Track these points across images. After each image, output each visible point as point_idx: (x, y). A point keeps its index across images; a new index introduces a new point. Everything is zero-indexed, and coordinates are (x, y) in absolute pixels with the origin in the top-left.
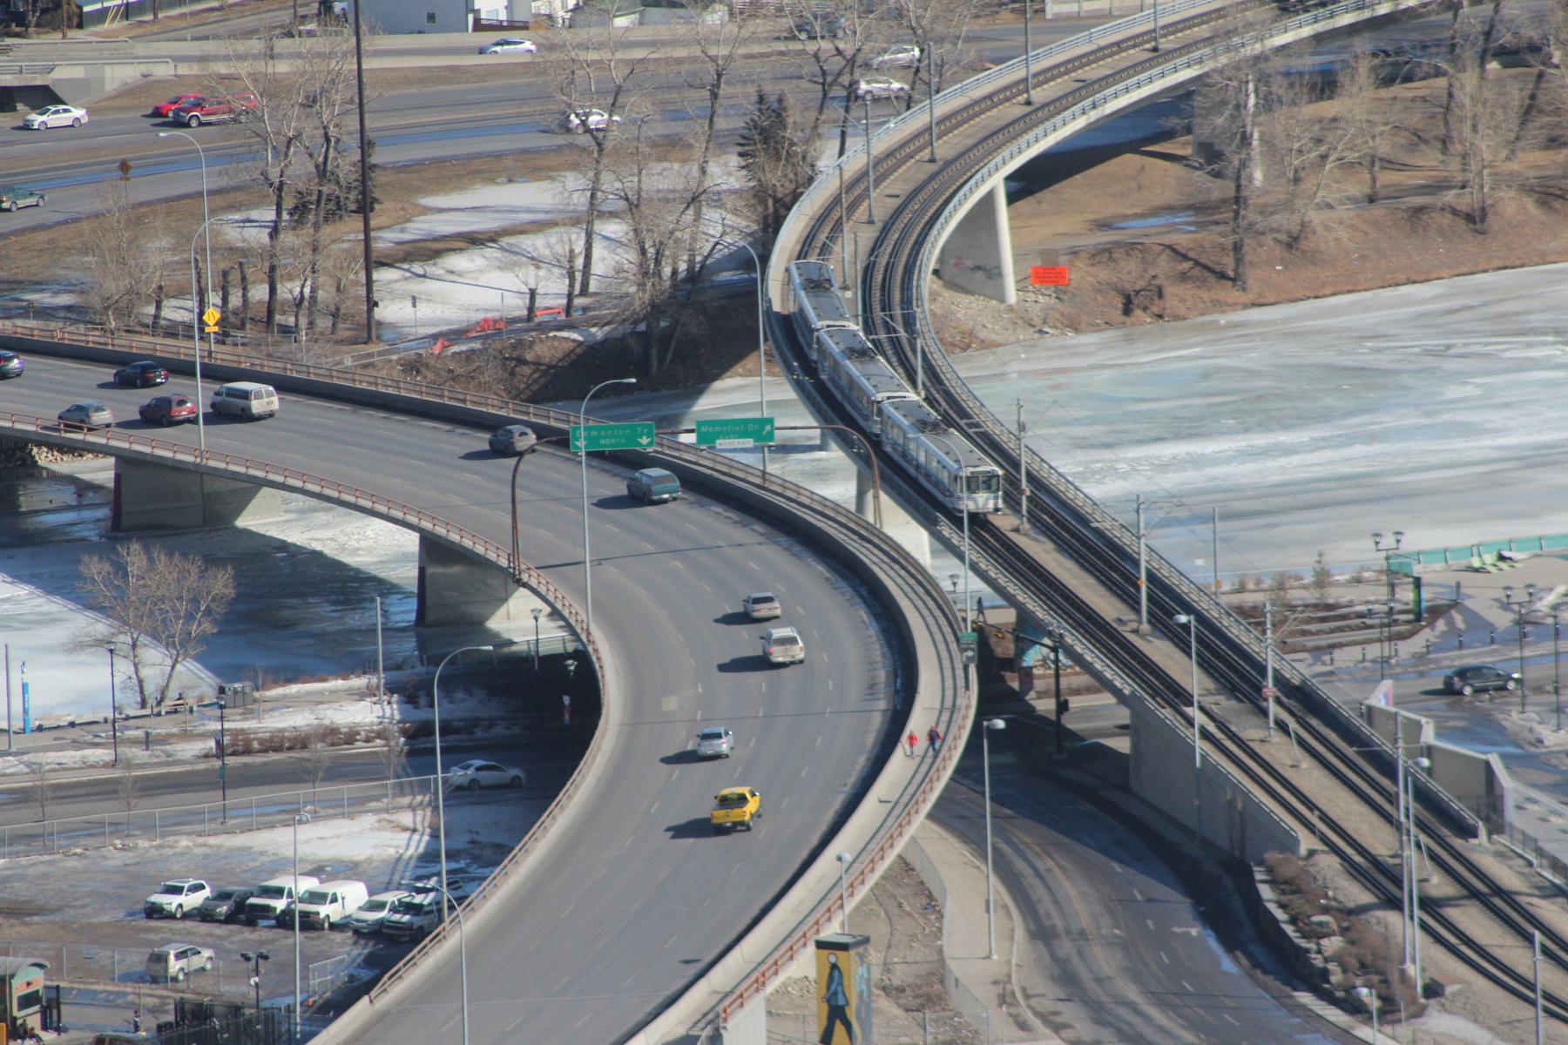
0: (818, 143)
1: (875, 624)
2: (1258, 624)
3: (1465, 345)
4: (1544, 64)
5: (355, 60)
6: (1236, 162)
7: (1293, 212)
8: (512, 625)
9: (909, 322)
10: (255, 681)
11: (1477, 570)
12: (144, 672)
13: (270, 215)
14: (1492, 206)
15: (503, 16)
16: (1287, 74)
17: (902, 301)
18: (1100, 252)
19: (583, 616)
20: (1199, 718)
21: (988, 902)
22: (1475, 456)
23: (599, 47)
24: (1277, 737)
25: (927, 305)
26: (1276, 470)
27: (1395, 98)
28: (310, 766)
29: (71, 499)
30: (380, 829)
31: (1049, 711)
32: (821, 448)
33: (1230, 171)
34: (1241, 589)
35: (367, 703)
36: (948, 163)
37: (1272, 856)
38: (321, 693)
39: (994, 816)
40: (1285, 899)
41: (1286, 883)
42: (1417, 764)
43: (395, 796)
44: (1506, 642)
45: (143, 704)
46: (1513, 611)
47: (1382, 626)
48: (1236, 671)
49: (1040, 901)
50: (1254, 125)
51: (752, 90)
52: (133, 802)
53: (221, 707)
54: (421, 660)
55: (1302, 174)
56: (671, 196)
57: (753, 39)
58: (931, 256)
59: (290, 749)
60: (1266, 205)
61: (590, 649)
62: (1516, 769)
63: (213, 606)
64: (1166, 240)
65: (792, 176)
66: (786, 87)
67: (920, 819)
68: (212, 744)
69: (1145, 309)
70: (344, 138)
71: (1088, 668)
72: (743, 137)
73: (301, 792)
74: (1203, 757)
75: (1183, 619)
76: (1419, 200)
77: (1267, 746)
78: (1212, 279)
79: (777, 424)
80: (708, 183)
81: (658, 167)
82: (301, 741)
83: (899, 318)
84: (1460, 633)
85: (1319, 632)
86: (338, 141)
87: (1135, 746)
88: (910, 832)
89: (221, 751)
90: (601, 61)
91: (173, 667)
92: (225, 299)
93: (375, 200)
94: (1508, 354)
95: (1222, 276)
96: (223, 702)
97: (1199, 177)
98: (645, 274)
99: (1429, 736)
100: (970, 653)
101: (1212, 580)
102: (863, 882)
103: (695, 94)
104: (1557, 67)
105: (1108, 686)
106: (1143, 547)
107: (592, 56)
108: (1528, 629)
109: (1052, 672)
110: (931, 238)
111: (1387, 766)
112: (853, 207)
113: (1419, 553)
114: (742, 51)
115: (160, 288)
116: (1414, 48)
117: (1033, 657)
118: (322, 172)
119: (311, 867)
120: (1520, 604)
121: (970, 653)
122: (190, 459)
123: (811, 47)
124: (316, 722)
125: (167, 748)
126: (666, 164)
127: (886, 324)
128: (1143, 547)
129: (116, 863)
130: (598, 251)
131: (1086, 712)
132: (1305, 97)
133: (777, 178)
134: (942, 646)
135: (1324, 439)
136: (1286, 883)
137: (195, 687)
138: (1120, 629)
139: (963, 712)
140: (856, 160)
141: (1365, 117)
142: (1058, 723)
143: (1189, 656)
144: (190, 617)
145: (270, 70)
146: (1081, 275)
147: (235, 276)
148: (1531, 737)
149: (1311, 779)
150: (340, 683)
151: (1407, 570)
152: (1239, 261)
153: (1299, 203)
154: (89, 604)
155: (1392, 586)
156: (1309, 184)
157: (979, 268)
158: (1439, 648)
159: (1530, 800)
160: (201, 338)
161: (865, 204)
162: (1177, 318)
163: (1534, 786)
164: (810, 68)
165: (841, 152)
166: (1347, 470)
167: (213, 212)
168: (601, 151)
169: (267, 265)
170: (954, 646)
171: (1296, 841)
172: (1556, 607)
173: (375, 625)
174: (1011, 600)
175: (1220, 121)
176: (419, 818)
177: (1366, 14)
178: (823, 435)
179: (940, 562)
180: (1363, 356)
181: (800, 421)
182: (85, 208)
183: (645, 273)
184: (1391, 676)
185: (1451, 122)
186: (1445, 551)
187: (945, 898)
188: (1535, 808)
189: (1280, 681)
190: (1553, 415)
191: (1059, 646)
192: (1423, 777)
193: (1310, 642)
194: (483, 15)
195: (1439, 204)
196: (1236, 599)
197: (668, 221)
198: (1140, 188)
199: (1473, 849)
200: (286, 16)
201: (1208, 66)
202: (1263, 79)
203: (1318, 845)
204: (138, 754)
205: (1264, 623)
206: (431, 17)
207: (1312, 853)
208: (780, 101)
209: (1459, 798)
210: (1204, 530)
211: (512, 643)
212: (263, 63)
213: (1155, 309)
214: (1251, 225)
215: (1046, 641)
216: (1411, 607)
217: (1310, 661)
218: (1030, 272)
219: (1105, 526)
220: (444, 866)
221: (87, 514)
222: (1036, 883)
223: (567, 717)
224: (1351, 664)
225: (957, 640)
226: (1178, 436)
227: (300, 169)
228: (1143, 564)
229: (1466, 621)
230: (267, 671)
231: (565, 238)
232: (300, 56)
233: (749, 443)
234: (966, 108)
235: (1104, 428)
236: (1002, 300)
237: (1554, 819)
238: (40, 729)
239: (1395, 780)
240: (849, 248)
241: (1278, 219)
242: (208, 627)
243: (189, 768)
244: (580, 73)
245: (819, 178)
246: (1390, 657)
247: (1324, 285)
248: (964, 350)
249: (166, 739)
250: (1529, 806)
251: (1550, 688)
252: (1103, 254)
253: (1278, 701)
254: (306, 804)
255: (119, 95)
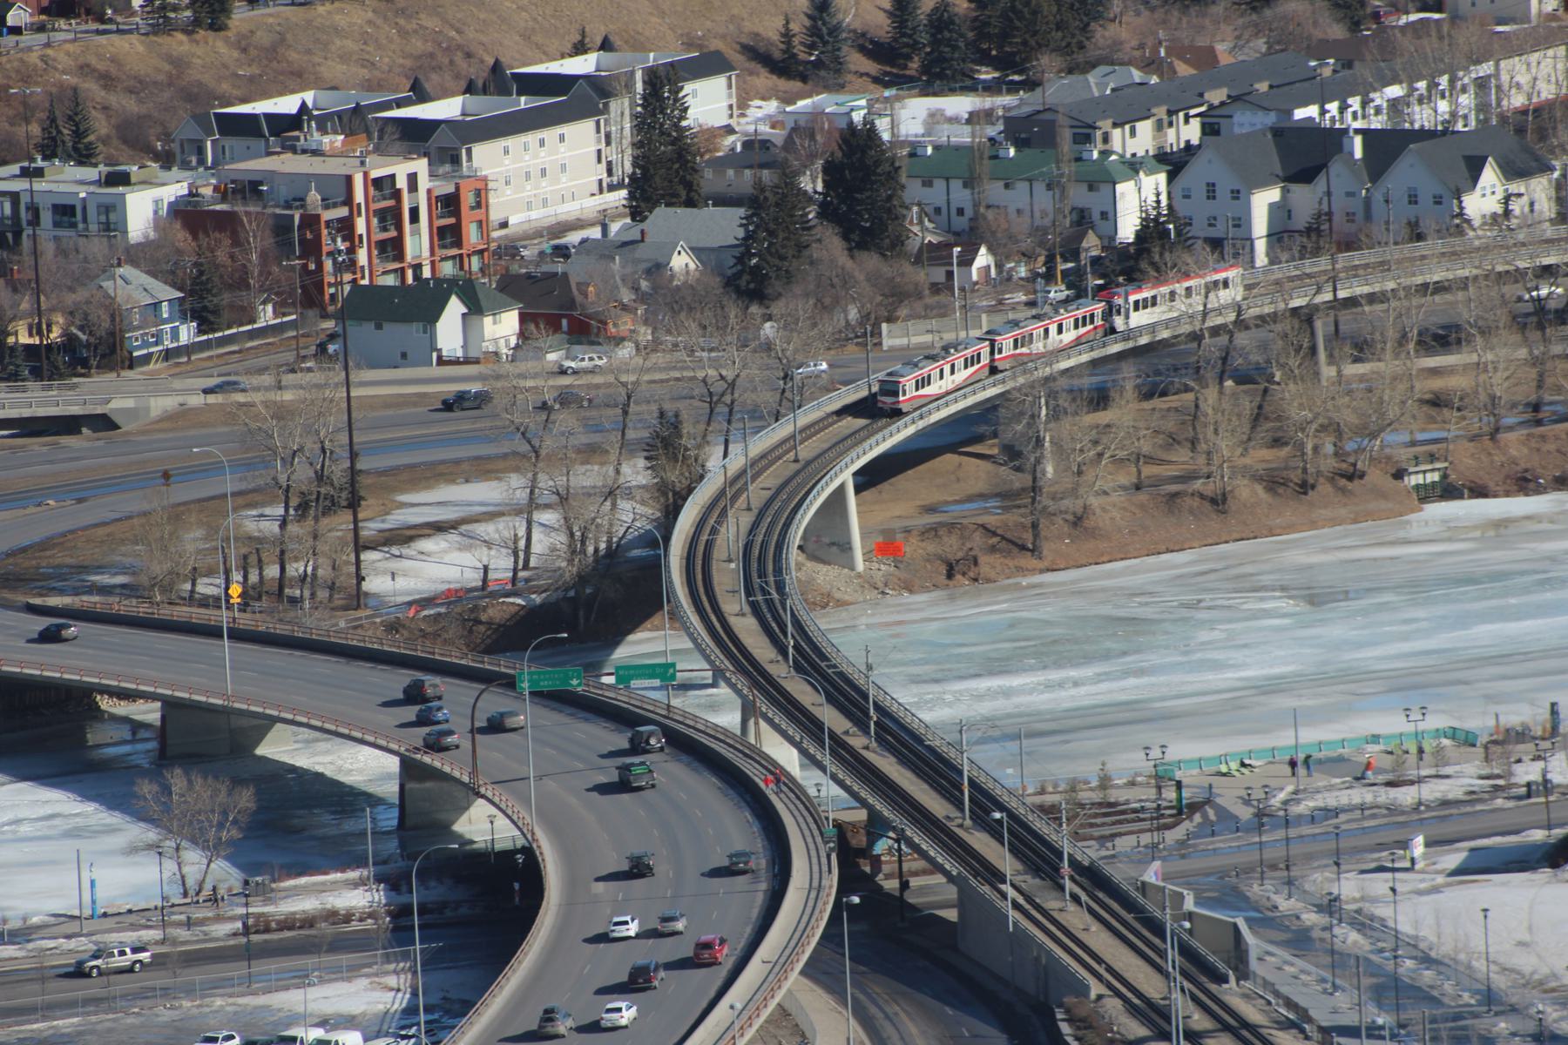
0: (707, 449)
1: (757, 823)
2: (1055, 819)
3: (1211, 599)
4: (1268, 382)
5: (345, 389)
6: (1032, 459)
7: (1077, 498)
8: (473, 828)
9: (780, 587)
10: (272, 875)
11: (1224, 775)
12: (186, 870)
13: (280, 511)
14: (1231, 491)
15: (460, 353)
16: (1071, 391)
17: (774, 570)
18: (928, 531)
19: (528, 820)
20: (1011, 893)
21: (848, 1039)
22: (1222, 685)
23: (535, 376)
24: (1072, 907)
25: (794, 573)
26: (1068, 698)
27: (1154, 409)
28: (316, 940)
29: (128, 735)
30: (373, 989)
31: (894, 889)
32: (713, 685)
33: (1028, 466)
34: (1042, 792)
35: (360, 891)
36: (808, 463)
37: (1069, 1000)
38: (323, 883)
39: (851, 972)
40: (1080, 1033)
41: (1080, 1020)
42: (1181, 926)
43: (383, 963)
44: (1248, 830)
45: (185, 894)
46: (1253, 806)
47: (1152, 819)
48: (1039, 856)
49: (889, 1038)
50: (1045, 431)
51: (654, 407)
52: (178, 971)
53: (247, 896)
54: (402, 856)
55: (1084, 468)
56: (592, 491)
57: (655, 368)
58: (796, 535)
59: (300, 928)
60: (1056, 493)
61: (535, 846)
62: (1261, 930)
63: (239, 817)
64: (980, 520)
65: (687, 474)
66: (681, 405)
67: (794, 975)
68: (239, 925)
69: (964, 574)
70: (337, 450)
71: (924, 855)
72: (648, 445)
73: (309, 961)
74: (1015, 924)
75: (997, 815)
76: (1174, 488)
77: (1064, 914)
78: (1015, 550)
79: (678, 668)
80: (622, 480)
81: (582, 469)
82: (309, 922)
83: (772, 584)
84: (1212, 824)
85: (1103, 824)
86: (332, 452)
87: (961, 915)
88: (787, 985)
89: (247, 930)
90: (536, 388)
91: (208, 866)
92: (245, 577)
93: (362, 498)
94: (1245, 607)
95: (1023, 548)
96: (248, 892)
97: (1004, 471)
98: (574, 552)
99: (1189, 904)
100: (832, 845)
101: (1019, 785)
102: (750, 1025)
103: (610, 412)
104: (1279, 384)
105: (940, 869)
106: (965, 760)
107: (530, 383)
108: (1265, 820)
109: (895, 858)
110: (796, 521)
111: (1158, 928)
112: (735, 498)
113: (1179, 762)
114: (646, 378)
115: (195, 569)
116: (1168, 370)
117: (881, 847)
118: (320, 477)
119: (317, 1020)
120: (1258, 800)
121: (832, 845)
122: (220, 702)
123: (700, 374)
124: (320, 907)
125: (205, 928)
126: (589, 467)
127: (762, 589)
128: (965, 760)
129: (165, 1019)
130: (536, 536)
131: (922, 890)
132: (1085, 410)
133: (674, 476)
134: (809, 840)
135: (1106, 673)
136: (1080, 1020)
137: (226, 880)
138: (948, 824)
139: (827, 890)
140: (736, 462)
141: (1132, 423)
142: (901, 899)
143: (1003, 844)
144: (221, 826)
145: (278, 398)
146: (913, 548)
147: (253, 559)
148: (1269, 905)
149: (1100, 939)
150: (338, 876)
151: (1171, 774)
152: (1036, 536)
153: (1082, 491)
154: (142, 817)
155: (1159, 788)
156: (1089, 475)
157: (833, 544)
158: (1197, 836)
159: (1268, 953)
160: (227, 608)
161: (745, 495)
162: (988, 581)
163: (1272, 942)
164: (699, 390)
165: (725, 455)
166: (1123, 697)
167: (235, 510)
168: (537, 457)
169: (278, 550)
170: (819, 839)
171: (1087, 987)
172: (1286, 802)
173: (366, 829)
174: (864, 803)
175: (1019, 428)
176: (402, 981)
177: (1130, 344)
178: (714, 675)
179: (807, 773)
180: (1133, 609)
181: (693, 666)
182: (135, 507)
183: (573, 552)
184: (1160, 858)
185: (1198, 427)
186: (1200, 760)
187: (815, 1037)
188: (1273, 959)
189: (1074, 863)
190: (1282, 653)
191: (901, 837)
192: (1185, 937)
193: (1096, 832)
194: (444, 353)
195: (1190, 491)
196: (1038, 800)
197: (590, 510)
198: (958, 480)
199: (1225, 992)
200: (290, 357)
201: (1009, 385)
202: (1053, 395)
203: (1104, 991)
204: (182, 934)
205: (1061, 818)
206: (404, 355)
207: (1100, 997)
208: (677, 416)
209: (1214, 953)
210: (1013, 746)
211: (473, 842)
212: (273, 393)
213: (972, 574)
214: (1045, 508)
215: (891, 834)
216: (1174, 803)
217: (1097, 847)
218: (873, 546)
219: (936, 743)
220: (422, 1018)
221: (140, 747)
222: (887, 1024)
223: (517, 899)
224: (1129, 849)
225: (822, 834)
226: (992, 673)
227: (303, 474)
228: (966, 773)
229: (1216, 814)
230: (282, 867)
231: (511, 524)
232: (301, 387)
233: (657, 682)
234: (822, 420)
235: (934, 667)
236: (852, 568)
237: (1287, 968)
238: (105, 915)
239: (1164, 940)
240: (733, 530)
241: (1067, 503)
242: (235, 833)
243: (221, 944)
244: (519, 397)
245: (709, 475)
246: (1159, 843)
247: (1102, 555)
248: (824, 607)
249: (202, 922)
250: (1268, 958)
251: (1282, 866)
252: (932, 532)
253: (1072, 879)
254: (313, 971)
255: (160, 420)
